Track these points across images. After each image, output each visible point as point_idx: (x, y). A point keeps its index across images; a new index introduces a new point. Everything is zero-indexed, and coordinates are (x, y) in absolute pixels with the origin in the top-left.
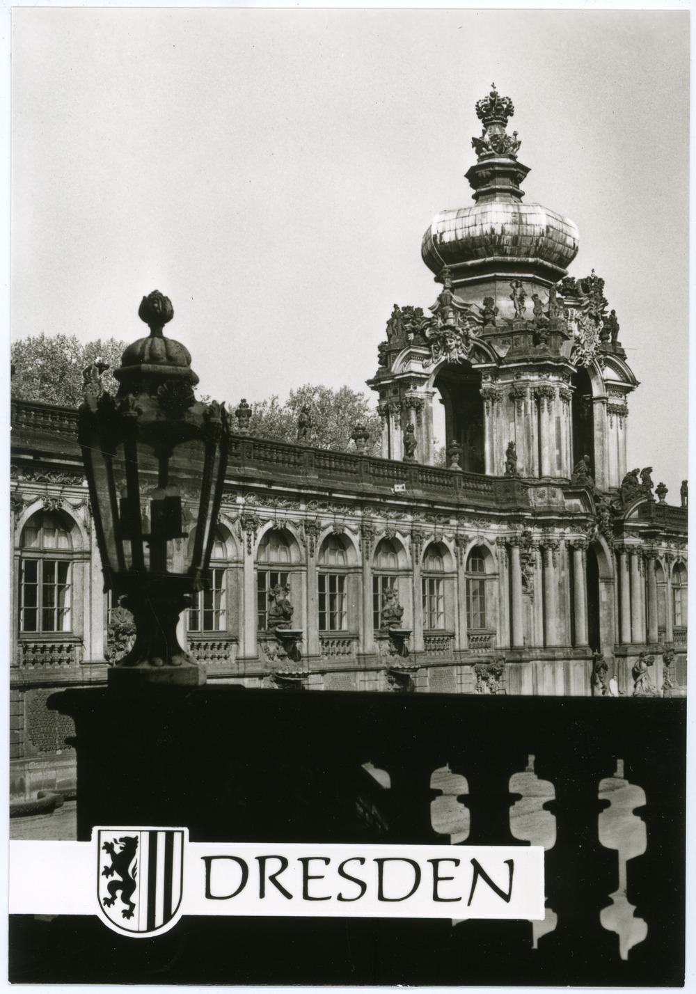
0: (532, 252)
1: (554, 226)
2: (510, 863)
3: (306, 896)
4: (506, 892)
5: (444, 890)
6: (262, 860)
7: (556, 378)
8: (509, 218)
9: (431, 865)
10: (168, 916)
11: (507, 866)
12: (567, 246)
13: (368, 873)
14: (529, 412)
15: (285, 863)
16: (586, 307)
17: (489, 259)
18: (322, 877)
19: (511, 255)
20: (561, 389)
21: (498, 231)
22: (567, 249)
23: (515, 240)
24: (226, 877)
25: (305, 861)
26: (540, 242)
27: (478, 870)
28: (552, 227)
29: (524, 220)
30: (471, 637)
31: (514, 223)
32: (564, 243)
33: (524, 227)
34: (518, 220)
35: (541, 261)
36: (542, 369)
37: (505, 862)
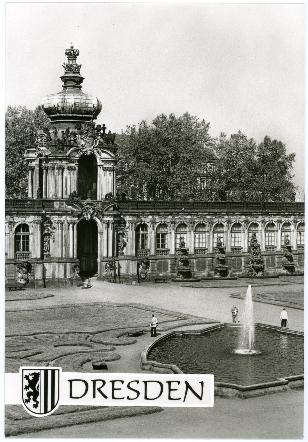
0: (71, 112)
1: (79, 102)
2: (202, 383)
3: (113, 397)
4: (200, 396)
5: (173, 395)
6: (94, 382)
7: (66, 162)
8: (60, 100)
9: (167, 384)
10: (53, 407)
11: (200, 384)
12: (89, 108)
13: (140, 387)
14: (56, 174)
15: (104, 383)
16: (86, 133)
17: (56, 115)
18: (120, 389)
19: (63, 113)
20: (67, 166)
21: (56, 106)
22: (89, 109)
23: (63, 108)
24: (78, 388)
25: (113, 382)
26: (72, 109)
27: (188, 386)
28: (78, 103)
29: (66, 101)
30: (18, 255)
31: (62, 102)
32: (87, 107)
33: (66, 104)
34: (64, 101)
35: (75, 115)
36: (61, 160)
37: (200, 383)
